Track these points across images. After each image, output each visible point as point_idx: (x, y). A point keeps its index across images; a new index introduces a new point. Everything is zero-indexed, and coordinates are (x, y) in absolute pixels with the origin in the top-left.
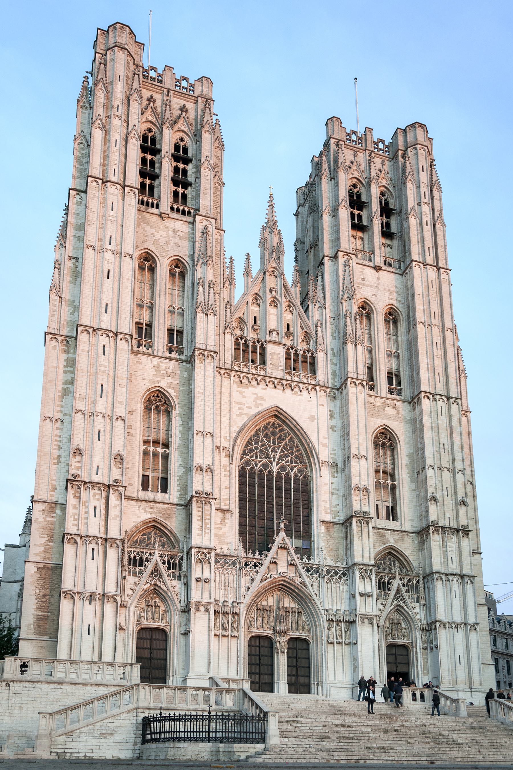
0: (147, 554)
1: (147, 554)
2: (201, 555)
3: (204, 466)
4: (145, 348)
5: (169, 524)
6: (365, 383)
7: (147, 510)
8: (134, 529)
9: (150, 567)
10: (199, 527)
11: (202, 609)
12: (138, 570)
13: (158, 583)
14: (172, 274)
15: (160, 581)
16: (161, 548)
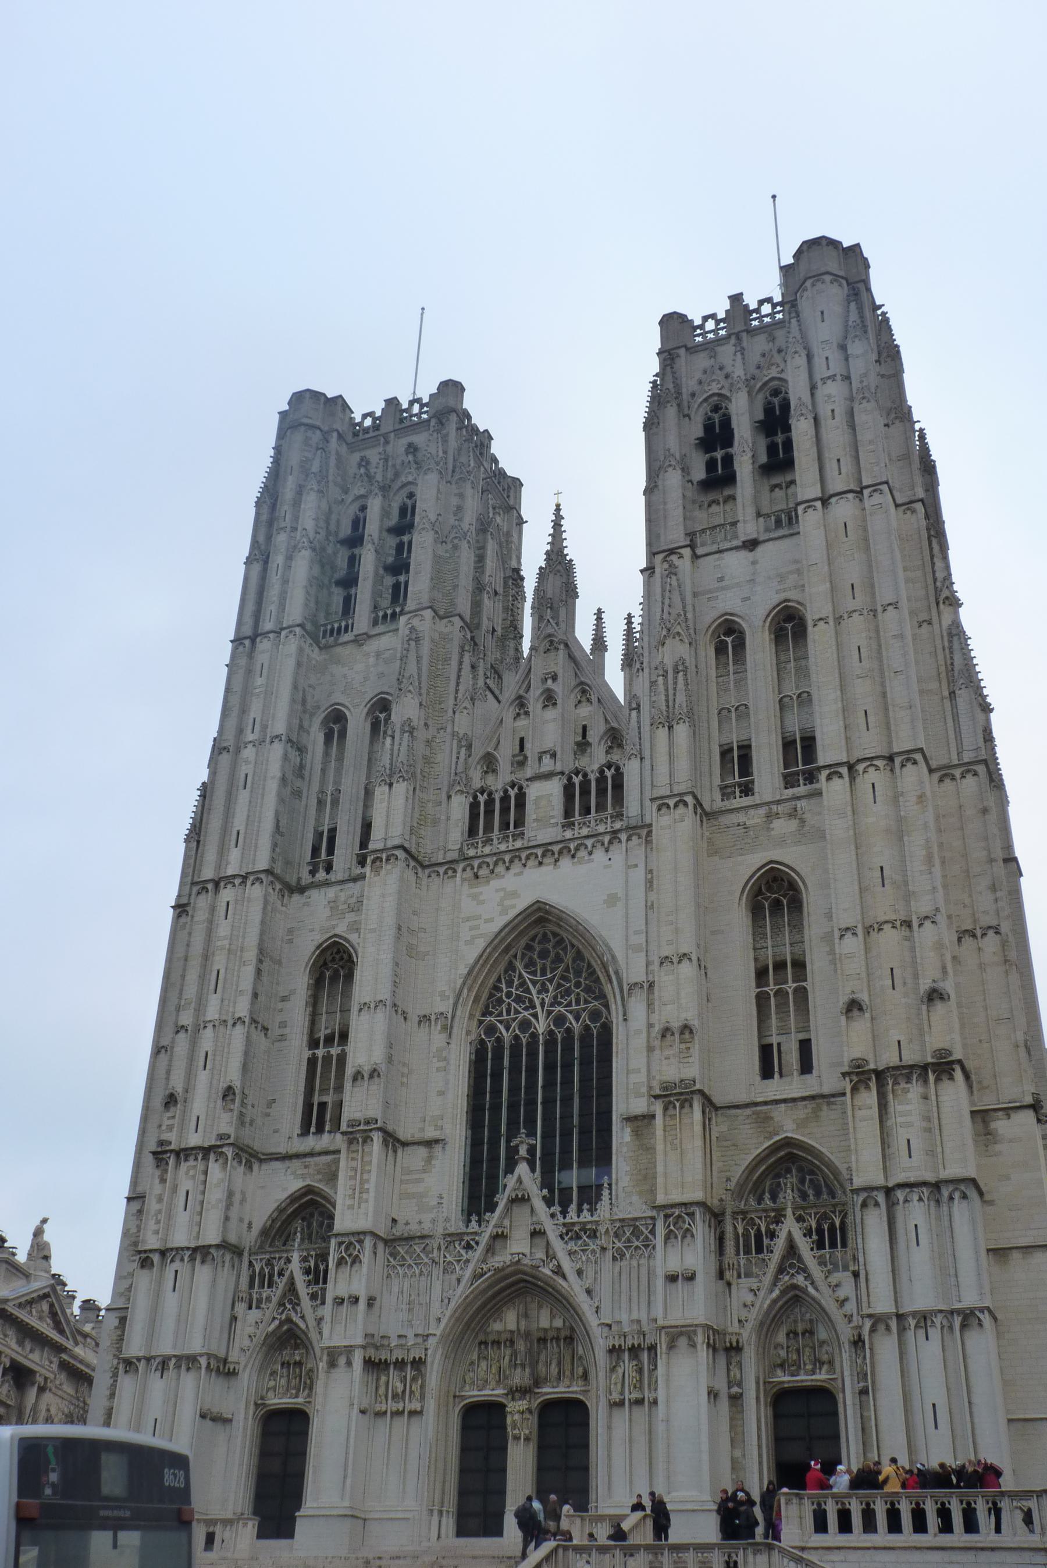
0: (282, 1261)
1: (282, 1261)
2: (347, 1249)
3: (366, 1070)
4: (324, 874)
5: (332, 1194)
6: (689, 799)
7: (299, 1172)
8: (275, 1215)
9: (281, 1283)
10: (351, 1192)
11: (342, 1360)
12: (264, 1296)
13: (293, 1314)
14: (375, 726)
15: (296, 1313)
16: (306, 1245)
